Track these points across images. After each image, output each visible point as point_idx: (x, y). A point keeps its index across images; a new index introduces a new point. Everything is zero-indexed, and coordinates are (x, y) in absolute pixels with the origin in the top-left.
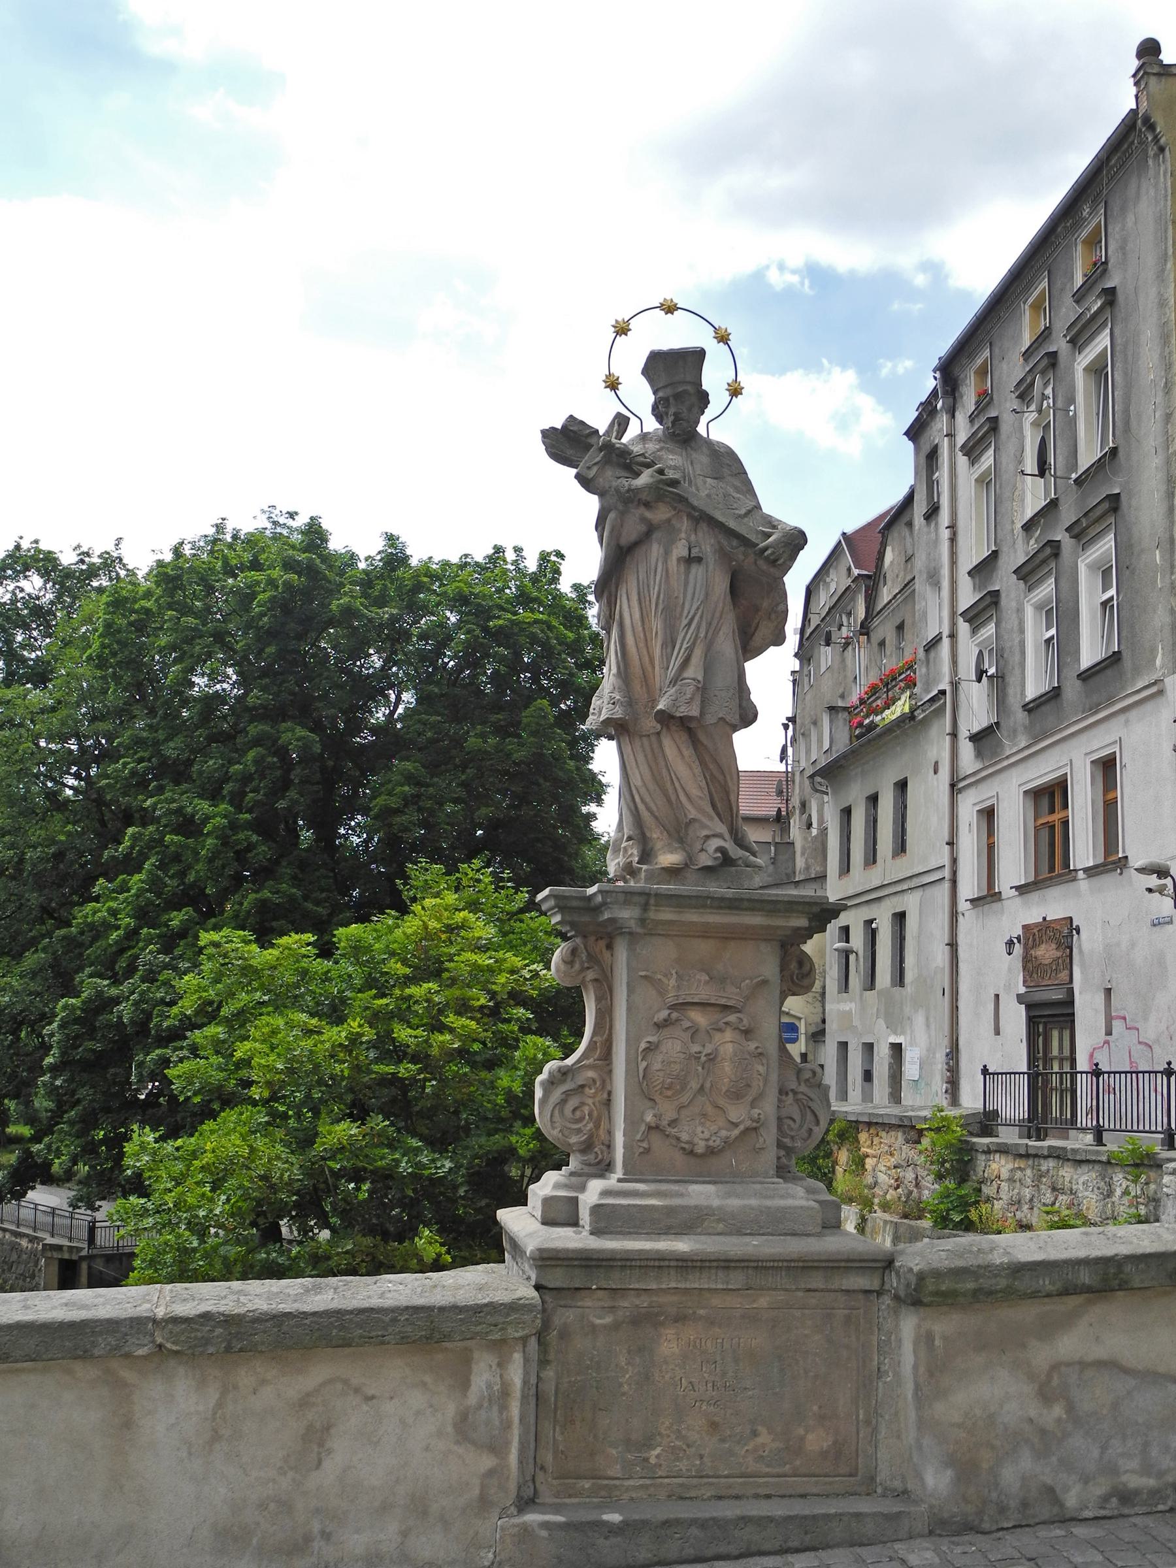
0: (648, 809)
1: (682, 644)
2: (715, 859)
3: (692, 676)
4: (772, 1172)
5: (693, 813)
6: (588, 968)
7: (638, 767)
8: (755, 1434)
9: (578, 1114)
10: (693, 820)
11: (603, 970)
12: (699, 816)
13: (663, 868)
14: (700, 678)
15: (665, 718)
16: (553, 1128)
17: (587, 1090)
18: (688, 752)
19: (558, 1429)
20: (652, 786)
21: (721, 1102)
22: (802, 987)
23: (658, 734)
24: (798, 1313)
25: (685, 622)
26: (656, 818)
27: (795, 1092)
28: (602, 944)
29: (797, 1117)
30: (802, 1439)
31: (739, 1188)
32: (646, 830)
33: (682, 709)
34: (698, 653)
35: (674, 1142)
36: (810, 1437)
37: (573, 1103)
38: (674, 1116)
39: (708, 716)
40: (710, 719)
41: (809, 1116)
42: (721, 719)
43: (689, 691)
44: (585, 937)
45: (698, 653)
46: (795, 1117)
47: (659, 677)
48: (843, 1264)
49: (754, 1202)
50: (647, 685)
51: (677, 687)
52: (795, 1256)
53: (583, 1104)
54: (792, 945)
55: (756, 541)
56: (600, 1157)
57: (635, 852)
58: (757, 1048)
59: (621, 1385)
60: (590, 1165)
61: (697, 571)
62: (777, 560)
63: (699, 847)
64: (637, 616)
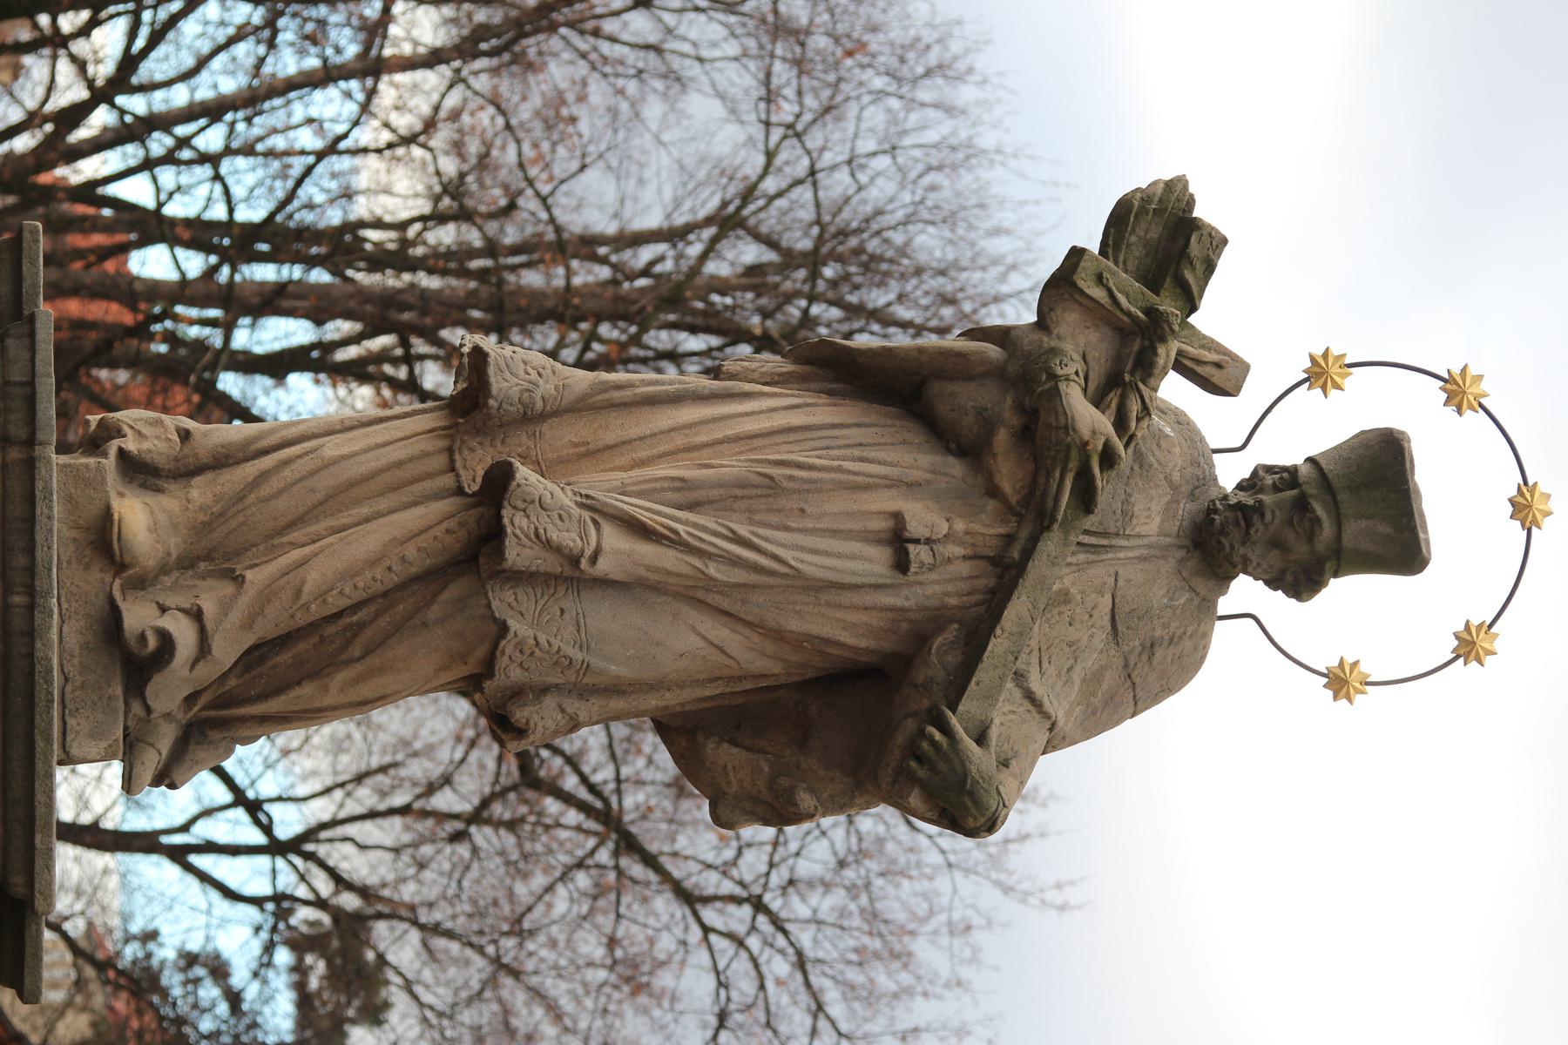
0: (264, 476)
1: (686, 523)
2: (142, 637)
3: (605, 545)
5: (256, 577)
7: (370, 449)
10: (239, 581)
12: (249, 593)
13: (107, 513)
14: (604, 566)
15: (499, 481)
18: (416, 558)
20: (325, 482)
23: (460, 491)
25: (743, 530)
26: (240, 497)
32: (209, 476)
33: (520, 520)
34: (667, 558)
39: (509, 596)
40: (502, 601)
42: (503, 629)
43: (568, 538)
45: (667, 558)
47: (602, 483)
50: (580, 456)
51: (576, 511)
55: (961, 708)
57: (146, 445)
61: (874, 562)
62: (920, 759)
63: (170, 601)
64: (751, 426)
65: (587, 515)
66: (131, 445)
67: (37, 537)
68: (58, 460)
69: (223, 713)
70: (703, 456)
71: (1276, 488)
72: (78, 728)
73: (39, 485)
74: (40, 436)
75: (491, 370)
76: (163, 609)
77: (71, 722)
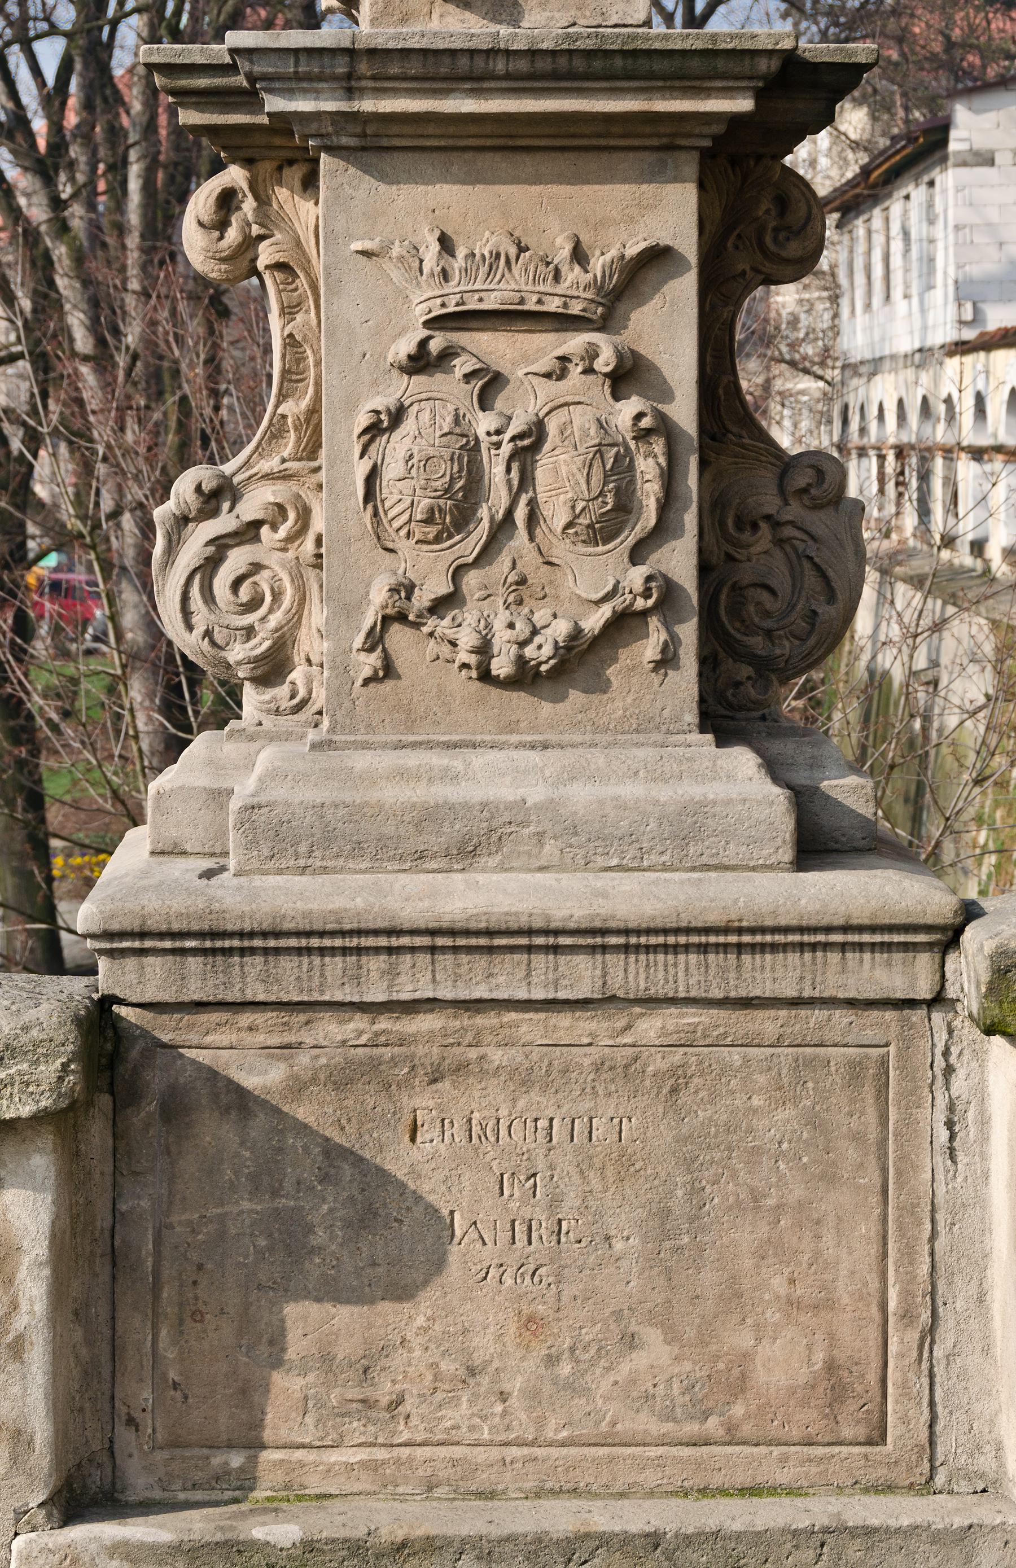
4: (691, 717)
6: (262, 238)
8: (631, 1342)
9: (245, 593)
11: (298, 244)
16: (190, 627)
17: (265, 530)
19: (164, 1333)
21: (561, 550)
22: (787, 261)
24: (735, 1056)
27: (775, 524)
28: (295, 174)
29: (780, 578)
30: (746, 1357)
31: (598, 758)
35: (446, 650)
36: (766, 1350)
37: (237, 560)
38: (443, 587)
41: (811, 580)
44: (248, 162)
46: (774, 583)
48: (837, 938)
49: (630, 790)
52: (713, 918)
53: (256, 567)
54: (759, 158)
56: (302, 693)
58: (639, 416)
59: (310, 1230)
60: (277, 712)
67: (442, 47)
72: (621, 13)
73: (391, 45)
74: (346, 44)
77: (614, 20)
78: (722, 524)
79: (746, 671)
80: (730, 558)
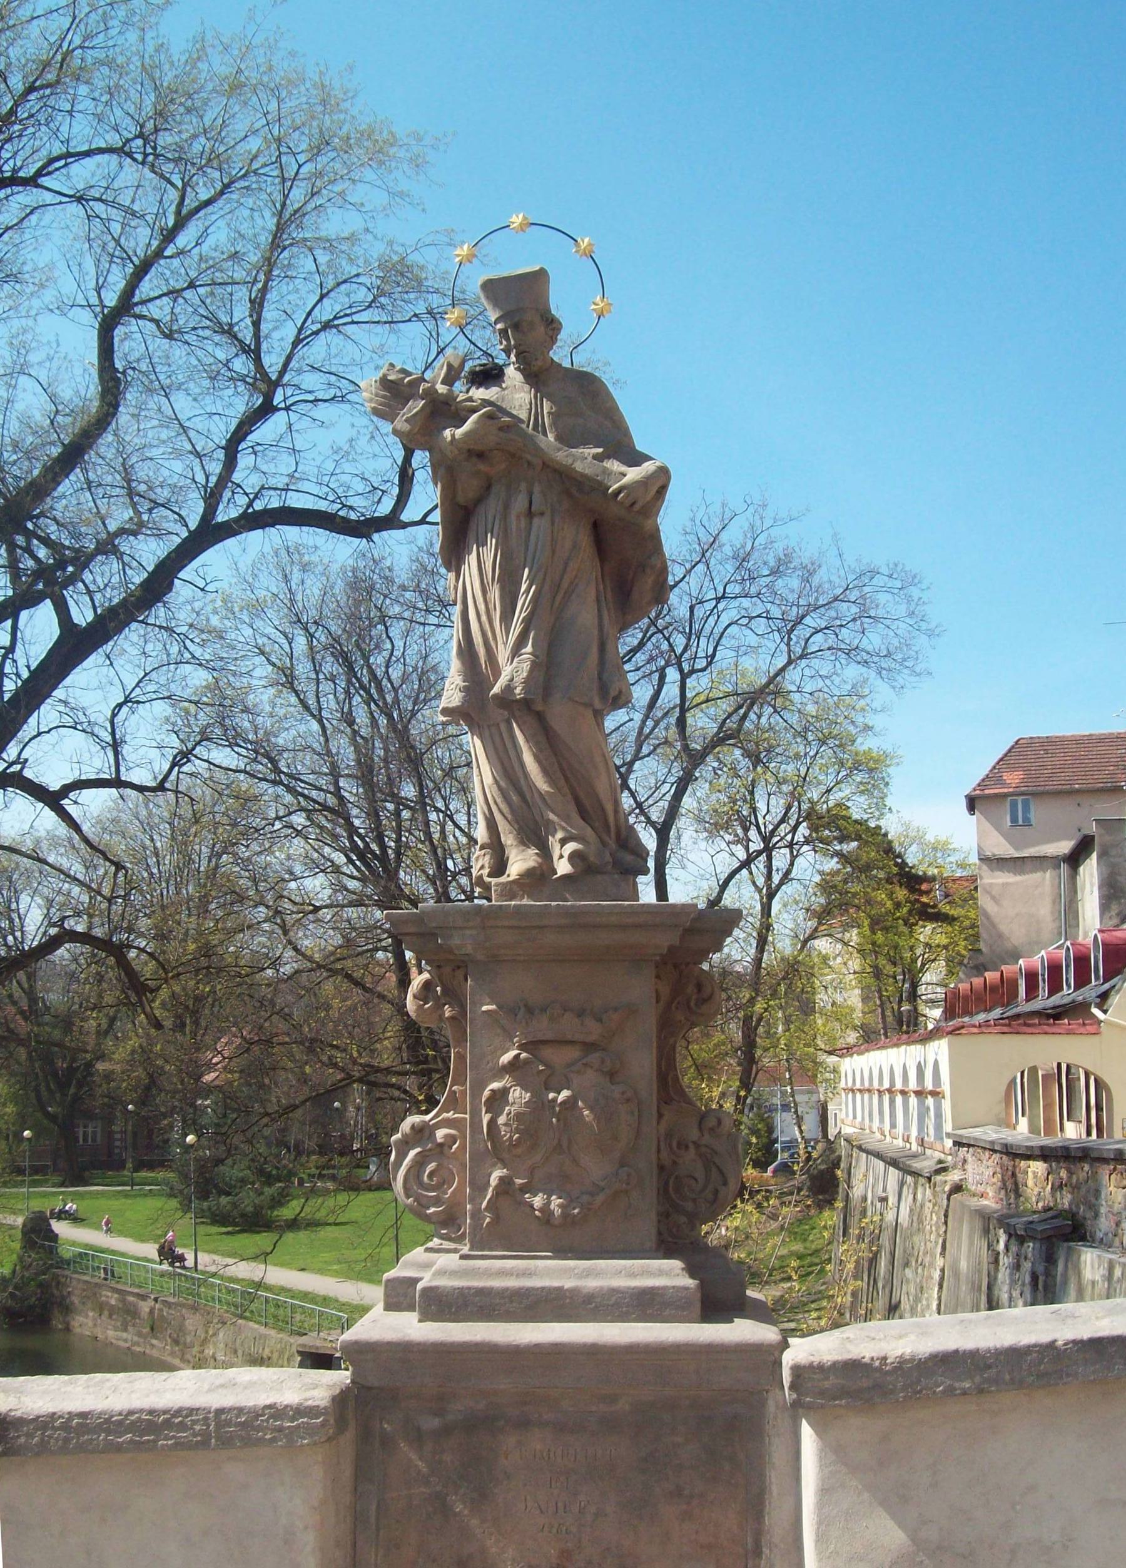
27: (697, 1145)
46: (697, 1175)
47: (503, 654)
54: (687, 964)
57: (487, 865)
65: (516, 660)
66: (486, 871)
68: (494, 902)
69: (613, 829)
70: (491, 606)
71: (508, 340)
75: (450, 705)
76: (561, 857)
78: (670, 1146)
79: (683, 1219)
80: (675, 1162)
